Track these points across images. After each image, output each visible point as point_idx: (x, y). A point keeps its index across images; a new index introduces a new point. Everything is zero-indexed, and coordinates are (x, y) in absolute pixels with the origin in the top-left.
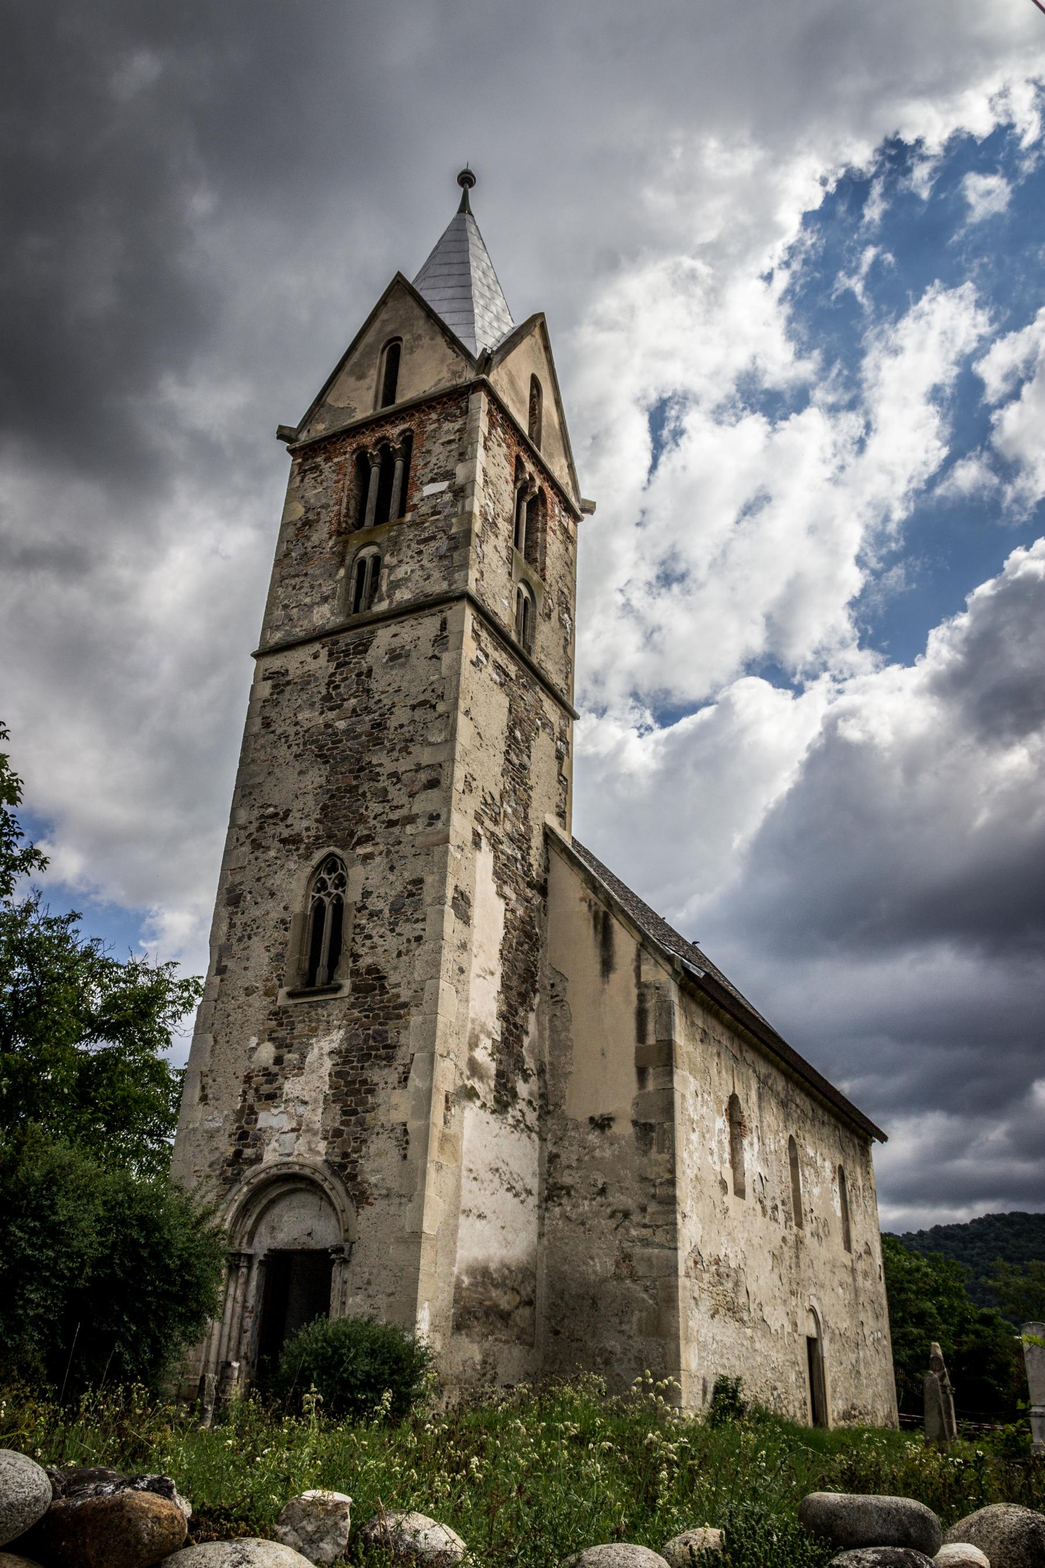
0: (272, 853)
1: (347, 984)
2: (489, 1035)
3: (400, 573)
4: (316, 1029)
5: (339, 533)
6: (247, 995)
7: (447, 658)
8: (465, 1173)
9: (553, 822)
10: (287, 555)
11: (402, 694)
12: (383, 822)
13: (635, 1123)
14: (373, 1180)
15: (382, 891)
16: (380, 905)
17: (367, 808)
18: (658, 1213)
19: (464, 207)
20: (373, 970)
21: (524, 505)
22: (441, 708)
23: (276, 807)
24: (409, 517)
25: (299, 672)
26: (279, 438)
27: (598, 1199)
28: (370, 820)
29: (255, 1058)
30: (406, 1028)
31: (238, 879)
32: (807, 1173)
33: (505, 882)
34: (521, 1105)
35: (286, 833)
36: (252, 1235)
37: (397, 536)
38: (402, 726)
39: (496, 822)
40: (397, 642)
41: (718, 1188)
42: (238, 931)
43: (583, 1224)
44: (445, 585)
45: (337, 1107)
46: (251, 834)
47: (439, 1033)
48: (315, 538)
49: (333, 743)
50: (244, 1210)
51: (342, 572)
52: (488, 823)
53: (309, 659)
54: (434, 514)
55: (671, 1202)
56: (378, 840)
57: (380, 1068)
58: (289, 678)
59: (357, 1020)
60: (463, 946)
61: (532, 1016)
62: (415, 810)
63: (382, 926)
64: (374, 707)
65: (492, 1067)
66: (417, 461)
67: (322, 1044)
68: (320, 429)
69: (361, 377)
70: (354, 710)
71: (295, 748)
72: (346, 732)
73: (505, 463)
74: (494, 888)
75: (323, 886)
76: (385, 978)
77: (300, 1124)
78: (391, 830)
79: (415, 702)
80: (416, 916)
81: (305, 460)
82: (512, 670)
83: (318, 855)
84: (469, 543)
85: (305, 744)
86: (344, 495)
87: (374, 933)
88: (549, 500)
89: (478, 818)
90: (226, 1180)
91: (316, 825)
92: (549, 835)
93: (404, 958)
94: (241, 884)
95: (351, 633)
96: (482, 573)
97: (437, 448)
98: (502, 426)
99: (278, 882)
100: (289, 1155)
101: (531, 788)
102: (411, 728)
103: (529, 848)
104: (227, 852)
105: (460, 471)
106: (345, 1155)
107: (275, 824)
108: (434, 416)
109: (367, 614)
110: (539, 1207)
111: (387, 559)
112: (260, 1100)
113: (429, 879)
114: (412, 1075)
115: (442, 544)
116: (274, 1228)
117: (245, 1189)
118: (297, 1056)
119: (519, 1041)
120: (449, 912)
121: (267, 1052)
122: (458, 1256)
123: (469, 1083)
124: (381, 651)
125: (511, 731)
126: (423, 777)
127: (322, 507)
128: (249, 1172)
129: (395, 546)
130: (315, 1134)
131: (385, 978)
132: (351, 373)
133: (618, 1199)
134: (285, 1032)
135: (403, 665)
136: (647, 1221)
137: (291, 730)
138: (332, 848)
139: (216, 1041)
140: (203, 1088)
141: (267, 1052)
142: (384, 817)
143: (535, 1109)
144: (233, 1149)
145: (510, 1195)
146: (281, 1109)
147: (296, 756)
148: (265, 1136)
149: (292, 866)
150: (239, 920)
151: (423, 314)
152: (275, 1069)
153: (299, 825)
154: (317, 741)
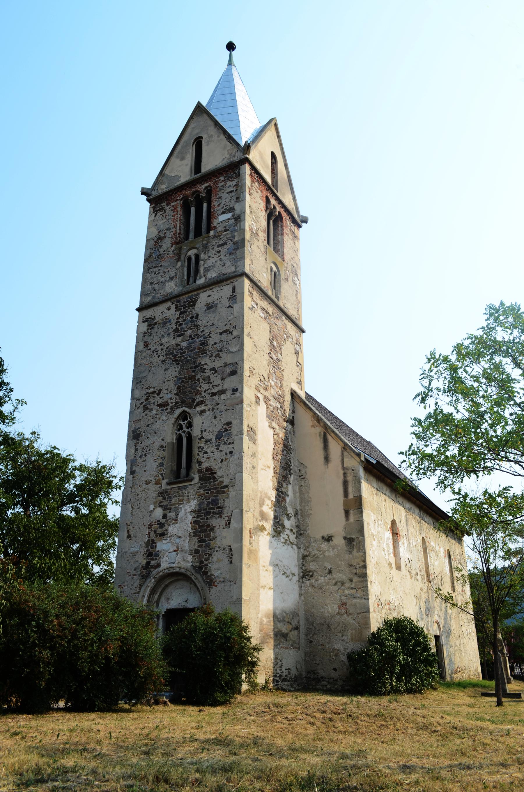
0: (154, 412)
1: (196, 477)
2: (269, 498)
3: (209, 263)
4: (182, 500)
5: (176, 243)
6: (147, 484)
7: (236, 307)
8: (261, 568)
9: (296, 388)
10: (150, 256)
11: (215, 327)
12: (209, 394)
13: (345, 538)
14: (216, 574)
15: (211, 429)
17: (200, 387)
18: (358, 582)
19: (230, 62)
20: (209, 469)
21: (271, 222)
22: (235, 333)
23: (154, 388)
24: (212, 233)
25: (161, 318)
26: (142, 194)
27: (328, 576)
28: (203, 393)
29: (153, 515)
30: (228, 498)
31: (138, 425)
32: (431, 555)
33: (273, 420)
34: (288, 532)
35: (160, 401)
36: (158, 602)
37: (207, 244)
38: (215, 344)
39: (266, 390)
40: (210, 300)
41: (387, 567)
42: (140, 452)
43: (321, 589)
44: (233, 269)
45: (196, 539)
46: (142, 403)
47: (244, 500)
48: (164, 247)
50: (153, 591)
51: (179, 264)
52: (262, 391)
53: (166, 311)
54: (225, 231)
55: (364, 576)
56: (207, 403)
57: (216, 518)
58: (156, 321)
59: (202, 495)
60: (254, 455)
61: (290, 487)
62: (225, 387)
63: (212, 447)
64: (201, 334)
65: (271, 514)
66: (215, 203)
67: (186, 507)
68: (163, 188)
69: (182, 159)
70: (190, 336)
71: (161, 357)
72: (187, 348)
73: (260, 201)
74: (267, 424)
75: (181, 428)
76: (215, 473)
77: (178, 548)
78: (213, 397)
79: (221, 331)
80: (229, 441)
81: (156, 205)
82: (270, 309)
83: (178, 412)
84: (244, 246)
85: (166, 355)
86: (178, 222)
87: (208, 451)
88: (284, 218)
89: (257, 389)
90: (143, 577)
91: (175, 396)
92: (294, 395)
93: (224, 463)
94: (139, 428)
95: (186, 296)
96: (252, 261)
97: (224, 195)
98: (258, 181)
99: (158, 427)
100: (173, 563)
101: (283, 371)
102: (220, 344)
103: (284, 401)
104: (131, 412)
105: (237, 207)
106: (201, 562)
107: (154, 397)
108: (222, 178)
109: (193, 286)
110: (299, 581)
111: (202, 256)
112: (157, 536)
113: (234, 422)
114: (232, 521)
115: (230, 245)
116: (168, 599)
117: (153, 580)
118: (174, 514)
119: (284, 500)
120: (245, 438)
121: (159, 513)
122: (260, 609)
123: (261, 524)
124: (203, 305)
125: (271, 342)
126: (228, 370)
127: (167, 229)
129: (206, 247)
130: (186, 552)
131: (215, 473)
132: (177, 157)
133: (338, 576)
134: (167, 502)
136: (353, 586)
137: (159, 348)
138: (184, 408)
139: (132, 508)
140: (128, 532)
142: (209, 391)
143: (294, 534)
144: (145, 561)
145: (284, 577)
146: (168, 540)
147: (162, 361)
148: (161, 554)
149: (164, 418)
150: (139, 446)
151: (213, 123)
152: (163, 521)
154: (173, 353)
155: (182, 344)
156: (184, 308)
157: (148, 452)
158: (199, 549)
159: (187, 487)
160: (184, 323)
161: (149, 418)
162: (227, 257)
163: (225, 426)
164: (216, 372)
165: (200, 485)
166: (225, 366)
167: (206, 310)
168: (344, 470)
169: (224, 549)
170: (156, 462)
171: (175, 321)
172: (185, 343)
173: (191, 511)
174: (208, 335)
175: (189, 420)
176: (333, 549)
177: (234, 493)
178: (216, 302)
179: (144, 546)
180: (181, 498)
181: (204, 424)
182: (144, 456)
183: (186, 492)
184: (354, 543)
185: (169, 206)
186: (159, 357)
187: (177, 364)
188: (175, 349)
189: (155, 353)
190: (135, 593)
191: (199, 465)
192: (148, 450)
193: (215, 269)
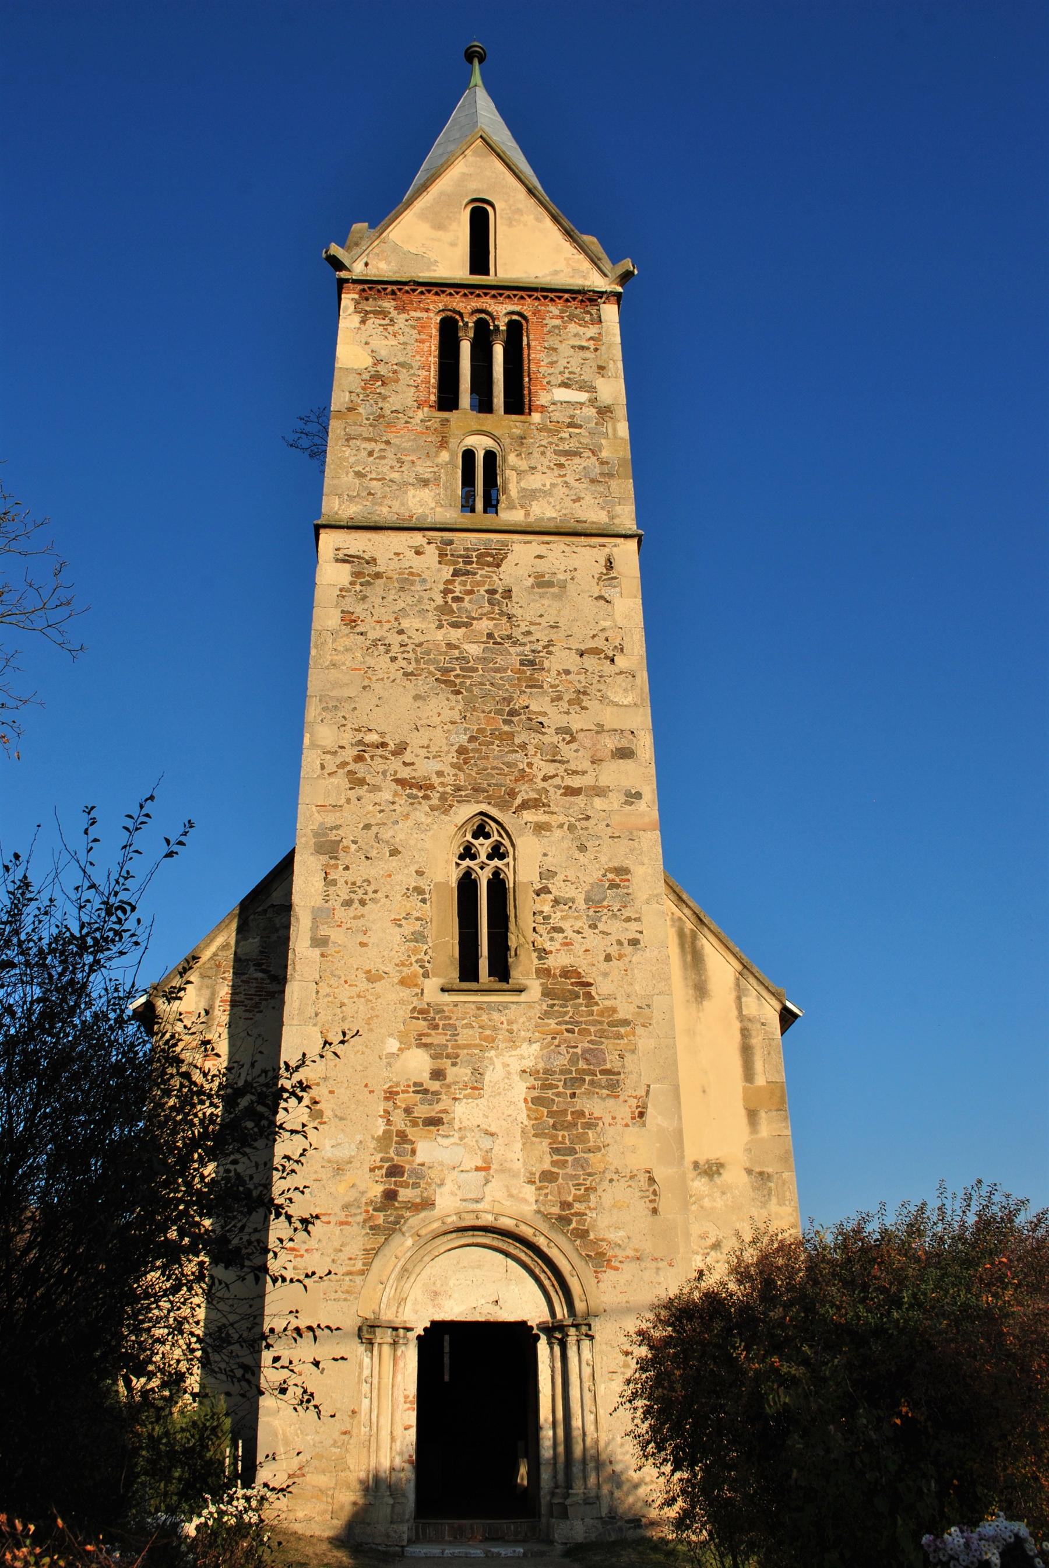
0: (386, 795)
3: (534, 481)
11: (562, 634)
12: (558, 787)
13: (749, 1172)
16: (569, 892)
20: (566, 973)
23: (382, 734)
24: (536, 417)
25: (394, 565)
27: (713, 1253)
28: (538, 780)
29: (397, 1065)
30: (633, 1051)
31: (330, 819)
35: (405, 773)
38: (567, 672)
40: (542, 566)
45: (545, 1144)
46: (344, 764)
48: (395, 402)
49: (461, 669)
51: (445, 456)
54: (571, 425)
57: (603, 1099)
62: (603, 781)
63: (576, 918)
67: (507, 1059)
70: (490, 636)
76: (591, 985)
79: (583, 647)
80: (626, 913)
83: (466, 811)
85: (417, 661)
87: (565, 925)
91: (454, 771)
94: (337, 827)
97: (564, 349)
99: (401, 836)
102: (582, 677)
108: (554, 309)
112: (415, 1124)
114: (650, 1111)
116: (436, 1294)
118: (468, 1071)
121: (418, 1064)
124: (523, 571)
126: (610, 743)
128: (415, 1220)
130: (515, 1175)
131: (591, 985)
132: (422, 216)
135: (557, 597)
137: (395, 639)
138: (484, 807)
141: (418, 1064)
152: (435, 1086)
153: (425, 768)
155: (466, 646)
156: (465, 563)
157: (371, 895)
158: (555, 1170)
159: (506, 1008)
160: (467, 598)
161: (371, 808)
162: (584, 486)
163: (610, 876)
164: (573, 740)
165: (545, 1007)
166: (598, 732)
167: (533, 587)
168: (741, 1021)
169: (632, 1177)
170: (400, 926)
171: (442, 587)
172: (475, 646)
173: (524, 1071)
174: (544, 647)
175: (496, 837)
176: (723, 1193)
177: (652, 1043)
178: (561, 576)
179: (372, 1144)
180: (488, 1032)
181: (549, 859)
182: (356, 904)
183: (503, 1019)
184: (772, 1185)
185: (405, 316)
186: (394, 659)
187: (458, 693)
188: (446, 653)
189: (382, 649)
190: (350, 1273)
191: (540, 958)
192: (370, 889)
193: (551, 500)
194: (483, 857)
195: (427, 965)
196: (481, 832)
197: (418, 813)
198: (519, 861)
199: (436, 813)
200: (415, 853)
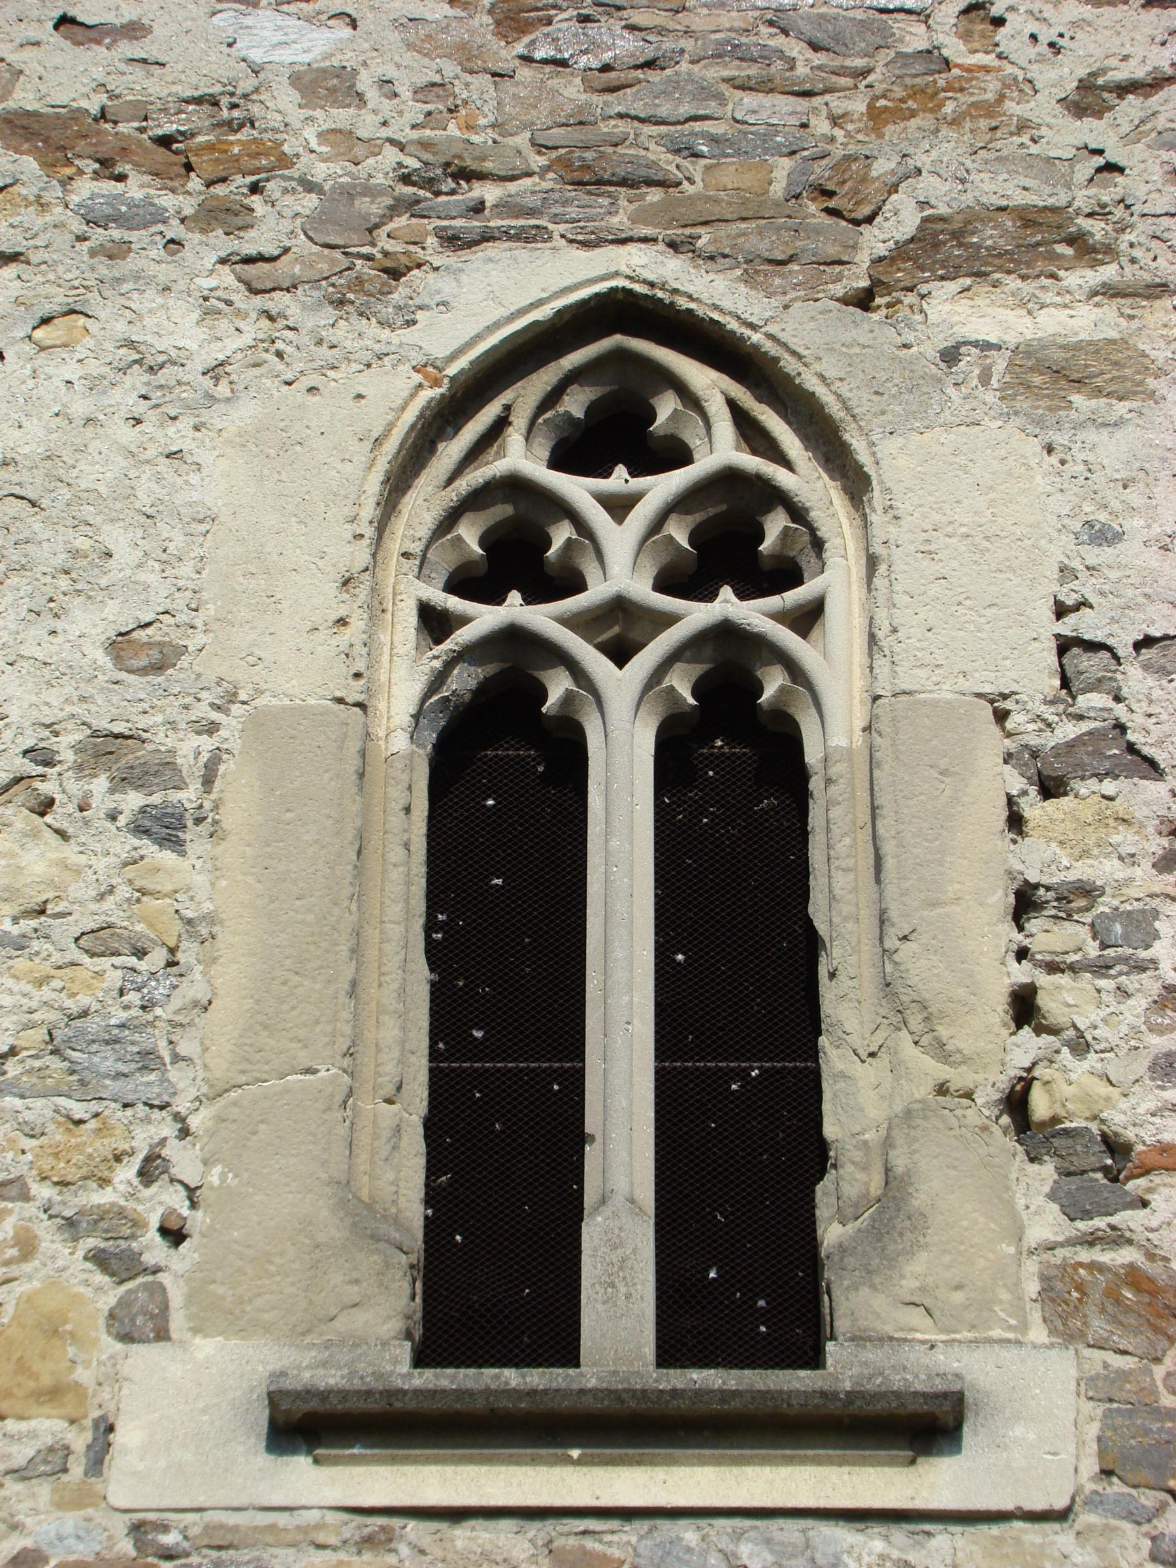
75: (518, 551)
194: (621, 567)
195: (154, 1249)
196: (615, 436)
197: (150, 300)
198: (905, 570)
199: (279, 301)
200: (117, 538)
